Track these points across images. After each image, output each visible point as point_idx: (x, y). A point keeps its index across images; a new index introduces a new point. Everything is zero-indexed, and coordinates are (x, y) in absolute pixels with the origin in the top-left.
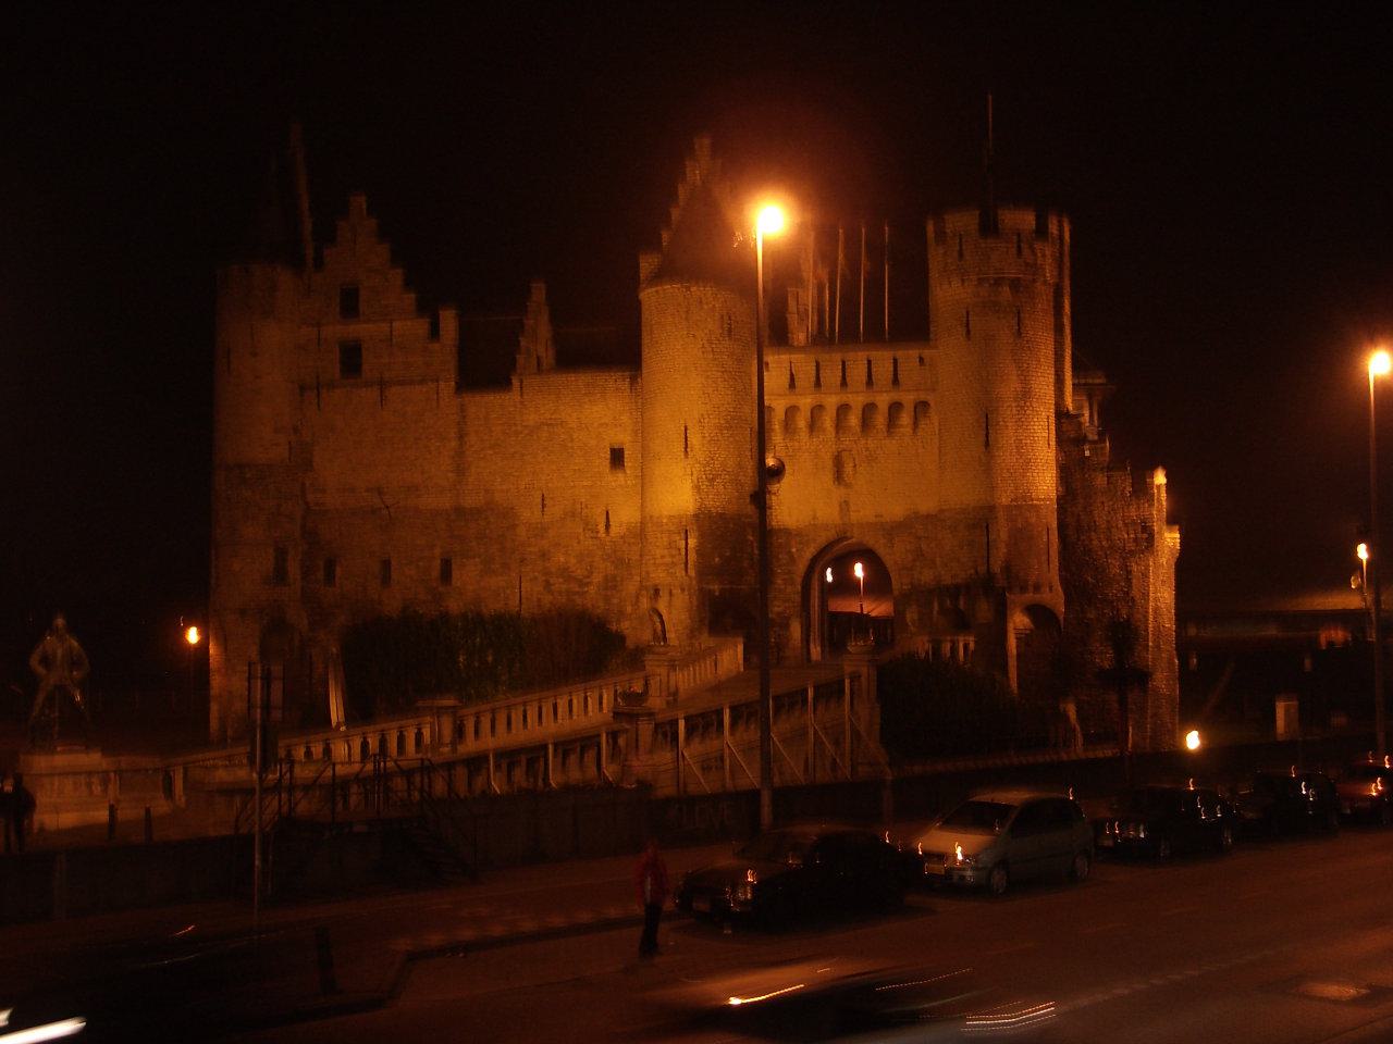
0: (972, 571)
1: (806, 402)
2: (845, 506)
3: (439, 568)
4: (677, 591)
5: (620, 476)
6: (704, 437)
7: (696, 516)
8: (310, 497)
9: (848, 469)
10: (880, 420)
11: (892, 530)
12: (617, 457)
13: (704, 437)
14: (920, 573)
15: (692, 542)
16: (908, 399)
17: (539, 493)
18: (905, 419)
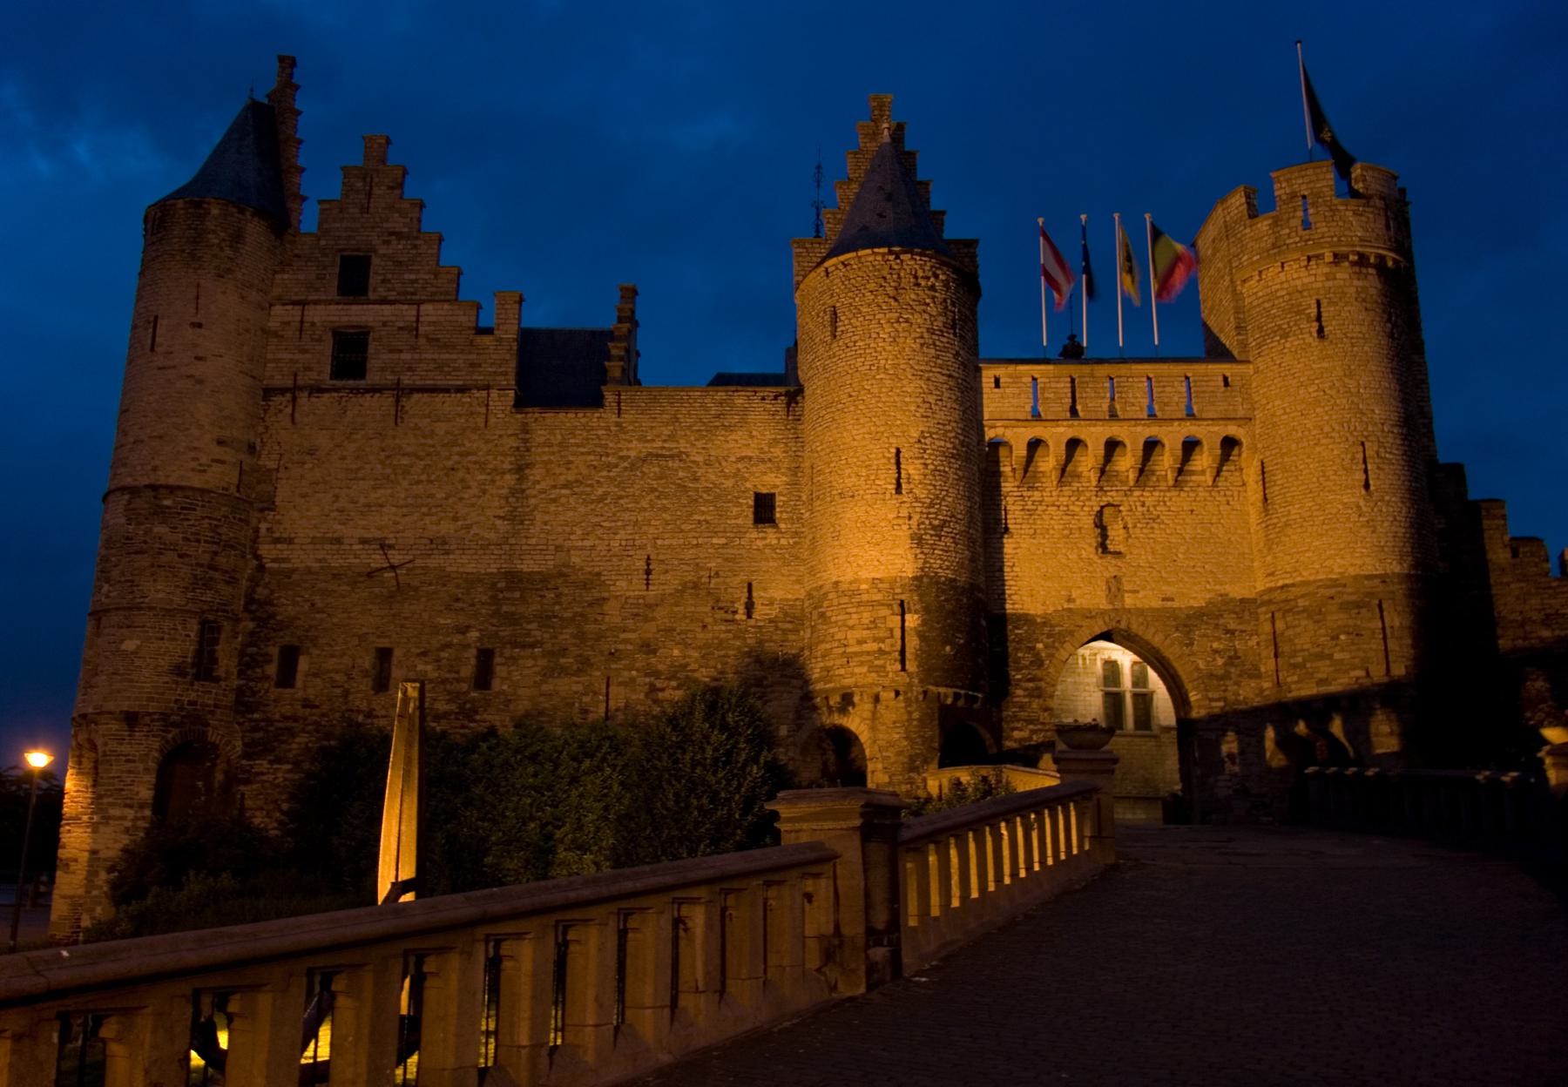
0: (1361, 673)
1: (1056, 435)
2: (1115, 587)
3: (473, 661)
4: (888, 696)
5: (770, 532)
6: (926, 465)
7: (915, 578)
8: (265, 550)
9: (1116, 533)
10: (1166, 462)
11: (1189, 622)
12: (764, 509)
13: (925, 464)
14: (1238, 684)
15: (912, 620)
16: (1210, 434)
17: (642, 554)
18: (1204, 461)
